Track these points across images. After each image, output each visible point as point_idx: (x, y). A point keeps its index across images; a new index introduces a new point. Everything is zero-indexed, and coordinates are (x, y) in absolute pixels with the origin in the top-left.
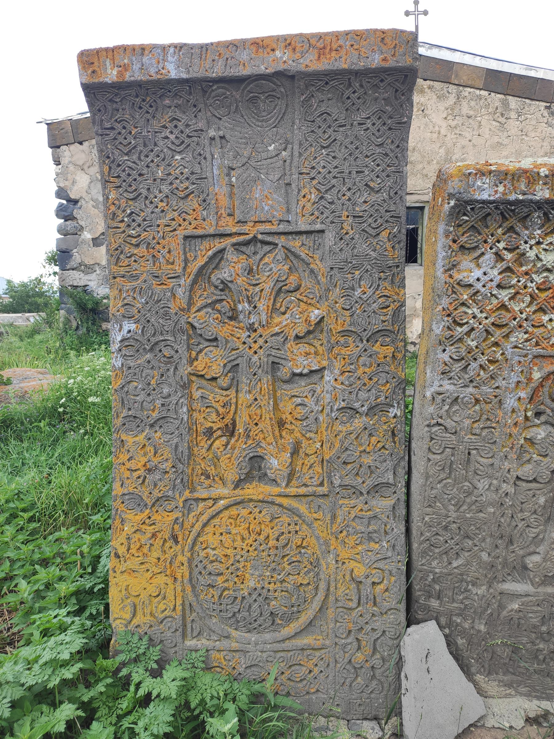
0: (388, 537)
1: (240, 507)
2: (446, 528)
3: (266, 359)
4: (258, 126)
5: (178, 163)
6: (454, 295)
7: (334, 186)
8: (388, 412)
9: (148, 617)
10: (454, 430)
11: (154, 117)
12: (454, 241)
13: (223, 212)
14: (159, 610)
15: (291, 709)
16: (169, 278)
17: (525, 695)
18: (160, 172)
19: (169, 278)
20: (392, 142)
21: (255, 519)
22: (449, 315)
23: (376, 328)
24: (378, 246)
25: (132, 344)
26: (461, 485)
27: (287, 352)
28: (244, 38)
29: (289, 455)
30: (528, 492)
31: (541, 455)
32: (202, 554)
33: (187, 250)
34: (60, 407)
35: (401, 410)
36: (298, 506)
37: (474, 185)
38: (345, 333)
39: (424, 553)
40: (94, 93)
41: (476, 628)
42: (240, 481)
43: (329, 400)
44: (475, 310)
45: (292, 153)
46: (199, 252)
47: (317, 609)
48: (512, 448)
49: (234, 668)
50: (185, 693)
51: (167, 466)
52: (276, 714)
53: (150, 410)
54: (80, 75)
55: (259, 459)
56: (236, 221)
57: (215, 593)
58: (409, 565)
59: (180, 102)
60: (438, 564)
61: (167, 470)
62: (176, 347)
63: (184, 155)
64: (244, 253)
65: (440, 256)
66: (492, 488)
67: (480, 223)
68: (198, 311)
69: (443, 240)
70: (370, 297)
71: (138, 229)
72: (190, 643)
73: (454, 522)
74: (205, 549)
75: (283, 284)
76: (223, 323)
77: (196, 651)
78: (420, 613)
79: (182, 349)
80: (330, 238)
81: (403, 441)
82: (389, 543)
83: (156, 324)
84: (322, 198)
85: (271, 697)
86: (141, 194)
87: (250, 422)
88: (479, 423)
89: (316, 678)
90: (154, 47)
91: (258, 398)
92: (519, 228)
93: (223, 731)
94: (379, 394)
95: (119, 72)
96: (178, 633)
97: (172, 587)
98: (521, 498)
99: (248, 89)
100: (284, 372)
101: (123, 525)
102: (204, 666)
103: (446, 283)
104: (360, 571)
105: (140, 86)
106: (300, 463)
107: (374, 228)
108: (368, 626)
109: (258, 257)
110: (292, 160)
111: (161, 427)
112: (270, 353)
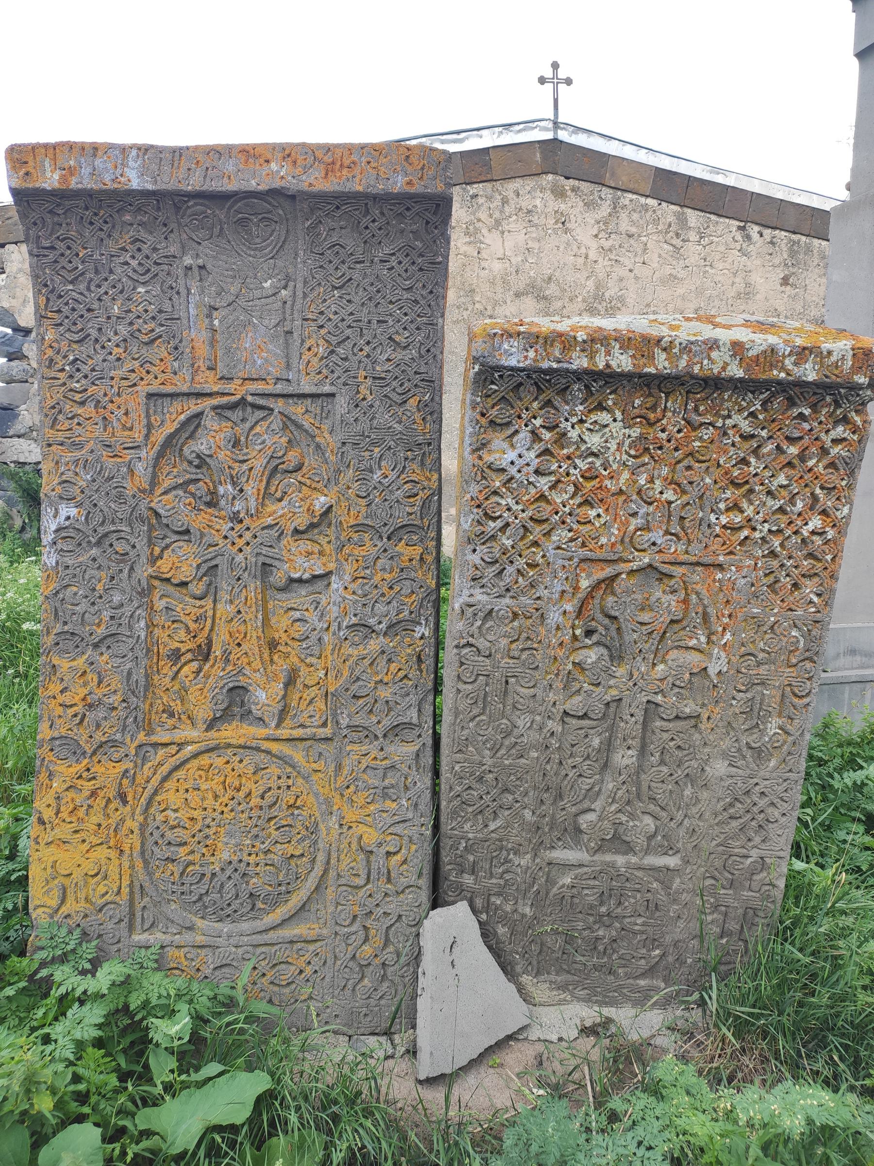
1: (213, 755)
2: (480, 779)
3: (254, 560)
7: (348, 338)
9: (83, 904)
11: (109, 236)
13: (201, 363)
14: (98, 894)
16: (125, 449)
17: (584, 1000)
18: (116, 307)
19: (125, 449)
20: (424, 286)
21: (233, 770)
22: (479, 506)
23: (400, 522)
24: (405, 417)
30: (580, 732)
31: (593, 685)
32: (160, 818)
33: (151, 412)
37: (500, 348)
38: (359, 528)
39: (454, 813)
40: (28, 201)
42: (215, 719)
44: (509, 500)
48: (557, 675)
51: (115, 699)
54: (9, 176)
55: (241, 692)
57: (175, 869)
59: (145, 219)
62: (133, 540)
65: (468, 432)
68: (165, 493)
71: (83, 382)
72: (139, 938)
74: (163, 811)
77: (147, 948)
79: (141, 543)
80: (341, 404)
83: (106, 510)
84: (332, 352)
86: (89, 335)
87: (231, 641)
90: (111, 146)
92: (557, 401)
96: (123, 924)
97: (117, 862)
98: (571, 738)
100: (278, 577)
101: (51, 780)
104: (371, 837)
105: (91, 196)
106: (296, 696)
111: (109, 647)
112: (259, 551)
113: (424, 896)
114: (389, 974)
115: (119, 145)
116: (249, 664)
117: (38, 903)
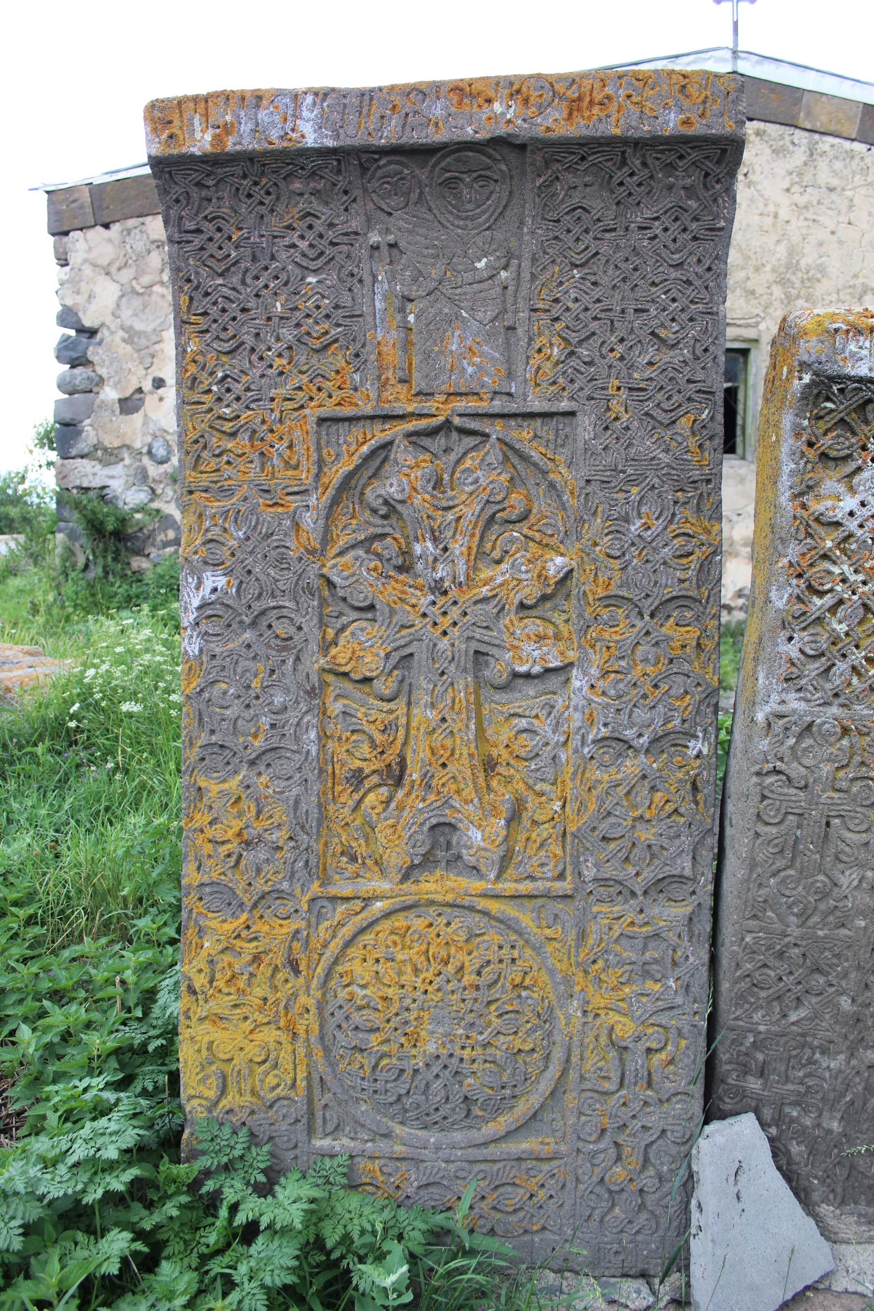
0: (677, 970)
1: (411, 914)
2: (781, 955)
3: (463, 646)
4: (458, 227)
5: (312, 289)
6: (808, 540)
7: (594, 334)
8: (687, 747)
9: (248, 1097)
10: (803, 783)
11: (272, 211)
12: (811, 445)
13: (390, 374)
15: (498, 1255)
18: (278, 305)
19: (288, 494)
20: (699, 261)
21: (438, 935)
22: (800, 576)
23: (668, 593)
25: (220, 613)
26: (811, 880)
27: (503, 633)
28: (437, 79)
29: (503, 822)
32: (343, 994)
33: (323, 442)
34: (71, 720)
35: (710, 744)
36: (517, 914)
38: (612, 601)
39: (741, 997)
40: (170, 173)
41: (825, 1125)
42: (413, 867)
43: (578, 724)
44: (845, 567)
45: (519, 274)
46: (345, 447)
47: (547, 1093)
49: (398, 1187)
50: (315, 1224)
51: (279, 836)
52: (474, 1263)
53: (249, 734)
54: (149, 142)
55: (447, 830)
56: (413, 392)
57: (365, 1062)
58: (712, 1019)
59: (320, 187)
60: (763, 1017)
61: (280, 844)
62: (299, 620)
63: (323, 276)
64: (427, 450)
66: (864, 885)
67: (854, 415)
68: (341, 554)
69: (791, 441)
70: (658, 535)
71: (235, 406)
72: (321, 1143)
73: (795, 945)
74: (347, 985)
75: (500, 507)
76: (387, 577)
77: (332, 1156)
78: (727, 1100)
79: (310, 624)
81: (711, 800)
82: (679, 982)
83: (263, 578)
84: (572, 353)
85: (464, 1234)
86: (243, 343)
88: (847, 770)
89: (541, 1207)
90: (279, 93)
91: (447, 717)
93: (384, 1285)
94: (670, 714)
95: (216, 137)
96: (300, 1126)
97: (289, 1048)
99: (443, 164)
100: (497, 671)
101: (201, 938)
102: (346, 1182)
103: (795, 517)
104: (625, 1028)
105: (251, 160)
106: (522, 837)
107: (666, 411)
108: (635, 1122)
109: (453, 457)
110: (518, 286)
111: (269, 765)
112: (471, 634)
113: (697, 1107)
114: (648, 1203)
115: (290, 92)
116: (458, 792)
117: (192, 1092)
